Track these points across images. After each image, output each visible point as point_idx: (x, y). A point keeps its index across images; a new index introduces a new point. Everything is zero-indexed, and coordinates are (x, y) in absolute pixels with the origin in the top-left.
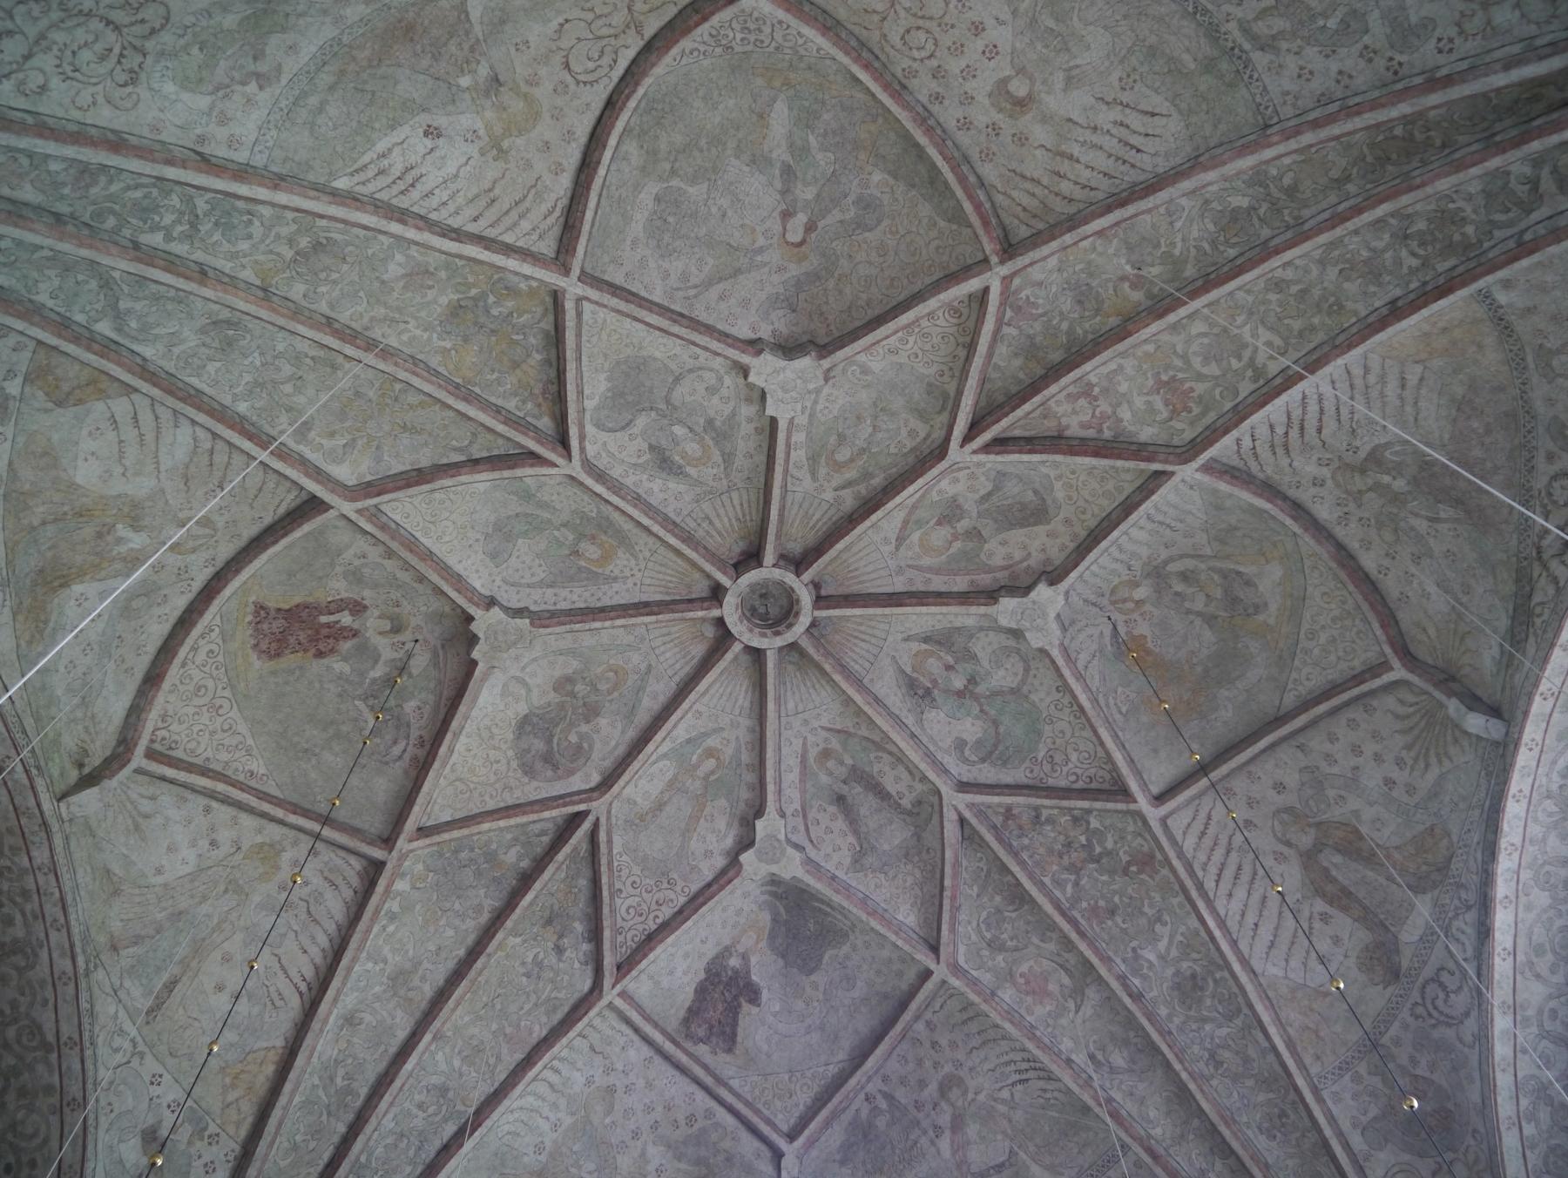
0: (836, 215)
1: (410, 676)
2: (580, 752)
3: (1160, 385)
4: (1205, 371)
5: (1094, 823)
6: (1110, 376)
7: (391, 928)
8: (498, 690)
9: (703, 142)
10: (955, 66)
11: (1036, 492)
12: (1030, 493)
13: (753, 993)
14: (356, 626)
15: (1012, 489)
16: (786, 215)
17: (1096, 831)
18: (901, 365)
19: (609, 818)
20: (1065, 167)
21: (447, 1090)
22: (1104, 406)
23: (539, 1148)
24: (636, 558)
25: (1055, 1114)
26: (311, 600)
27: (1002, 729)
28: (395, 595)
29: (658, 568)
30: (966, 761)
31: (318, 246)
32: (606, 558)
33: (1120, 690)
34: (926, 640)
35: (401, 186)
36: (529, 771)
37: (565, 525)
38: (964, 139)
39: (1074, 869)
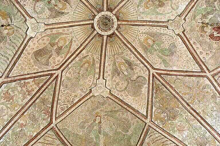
0: (89, 124)
1: (202, 14)
3: (12, 98)
6: (24, 98)
8: (180, 8)
9: (118, 140)
11: (38, 61)
12: (39, 60)
14: (213, 30)
15: (44, 60)
16: (100, 122)
18: (74, 92)
22: (24, 89)
24: (139, 39)
28: (201, 38)
33: (7, 5)
34: (63, 13)
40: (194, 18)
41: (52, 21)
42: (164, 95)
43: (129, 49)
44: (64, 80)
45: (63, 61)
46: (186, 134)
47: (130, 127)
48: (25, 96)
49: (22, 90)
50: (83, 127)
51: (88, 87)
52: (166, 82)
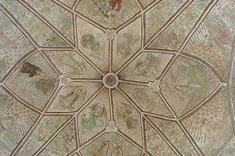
0: (181, 94)
2: (85, 46)
4: (161, 153)
5: (73, 140)
6: (157, 138)
7: (58, 9)
8: (99, 32)
10: (209, 112)
13: (30, 76)
16: (181, 86)
17: (72, 141)
19: (73, 51)
20: (194, 129)
21: (24, 17)
23: (7, 34)
25: (15, 137)
26: (122, 3)
27: (88, 122)
29: (119, 62)
30: (82, 116)
31: (192, 17)
32: (122, 53)
35: (199, 30)
36: (83, 37)
37: (129, 47)
38: (196, 114)
39: (64, 137)
40: (106, 22)
41: (108, 116)
42: (159, 41)
43: (127, 65)
44: (148, 110)
45: (135, 110)
46: (185, 27)
47: (183, 65)
48: (156, 137)
49: (152, 139)
50: (183, 99)
51: (154, 94)
52: (149, 40)
